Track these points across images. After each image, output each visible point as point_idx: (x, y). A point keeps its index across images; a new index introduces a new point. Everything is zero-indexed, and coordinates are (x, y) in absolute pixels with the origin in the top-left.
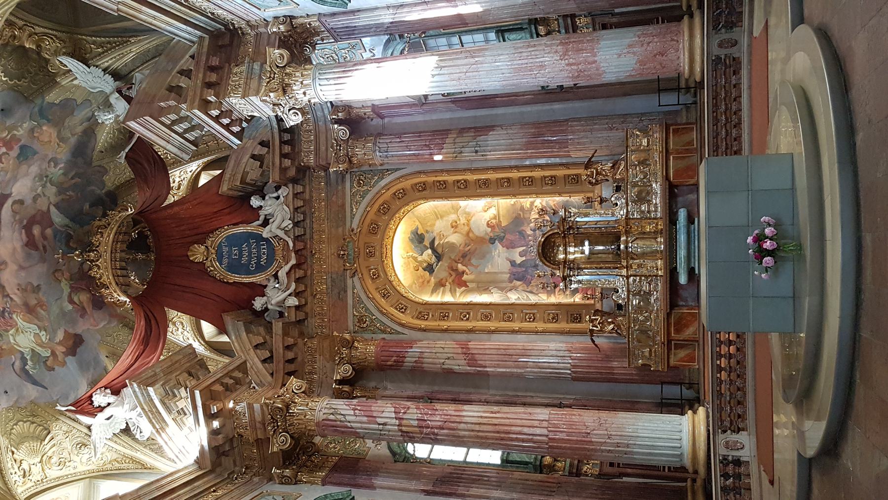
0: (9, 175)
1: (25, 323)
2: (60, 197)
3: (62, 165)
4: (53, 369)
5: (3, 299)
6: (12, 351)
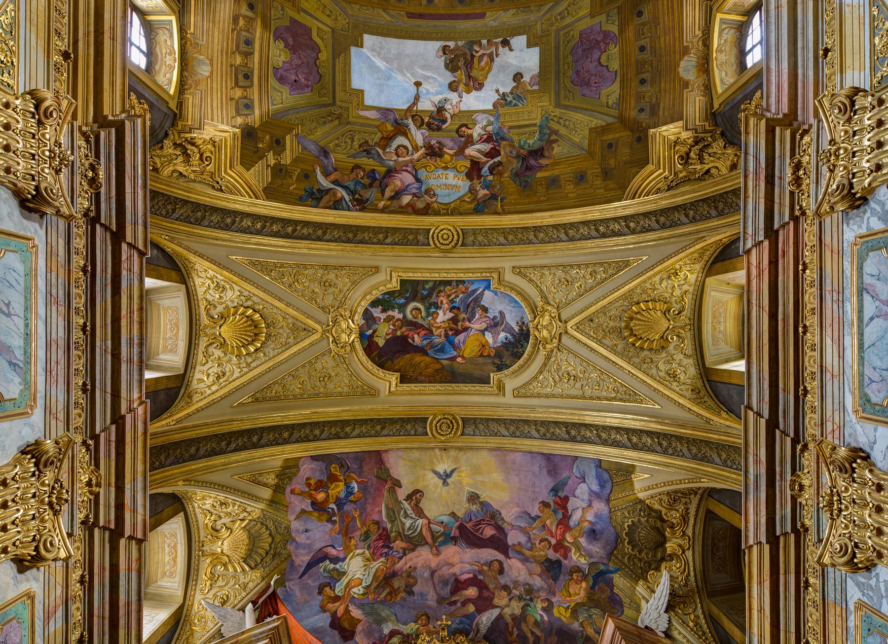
0: (528, 553)
1: (374, 570)
2: (509, 619)
3: (546, 618)
4: (320, 593)
5: (401, 548)
6: (348, 549)
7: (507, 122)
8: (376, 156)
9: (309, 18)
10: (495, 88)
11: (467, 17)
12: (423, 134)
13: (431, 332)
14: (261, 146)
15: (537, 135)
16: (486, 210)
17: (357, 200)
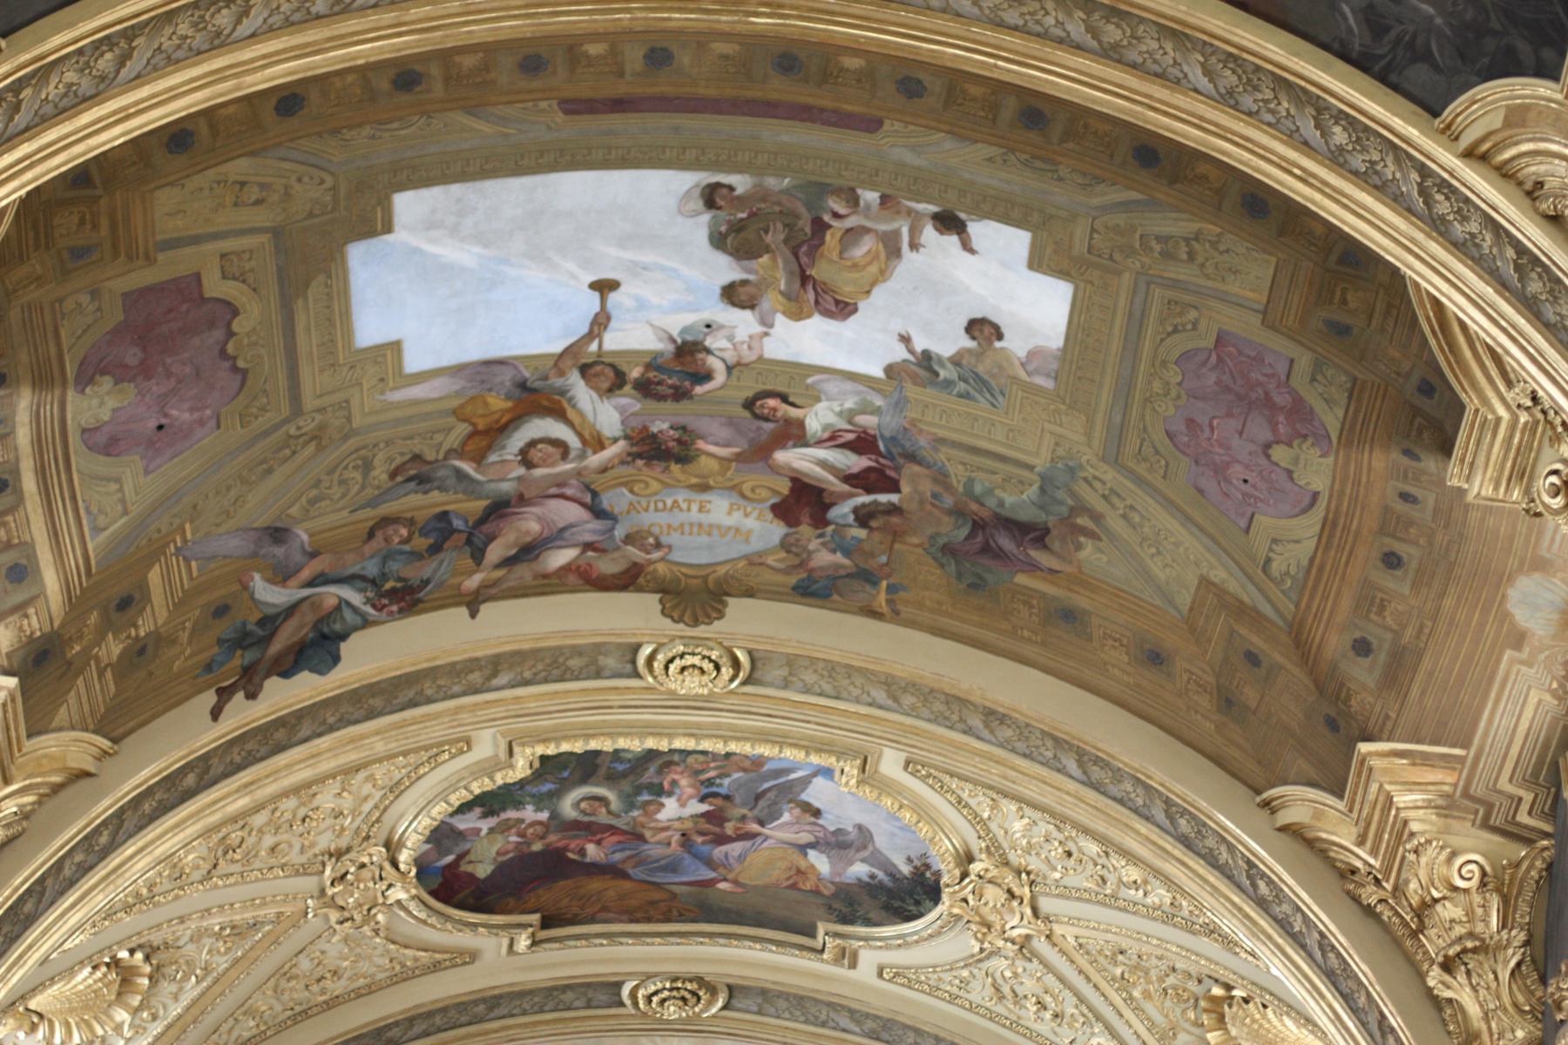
7: (929, 424)
8: (451, 481)
9: (188, 250)
10: (898, 326)
11: (804, 114)
12: (621, 410)
13: (641, 838)
14: (77, 648)
15: (1032, 492)
16: (835, 597)
17: (392, 593)
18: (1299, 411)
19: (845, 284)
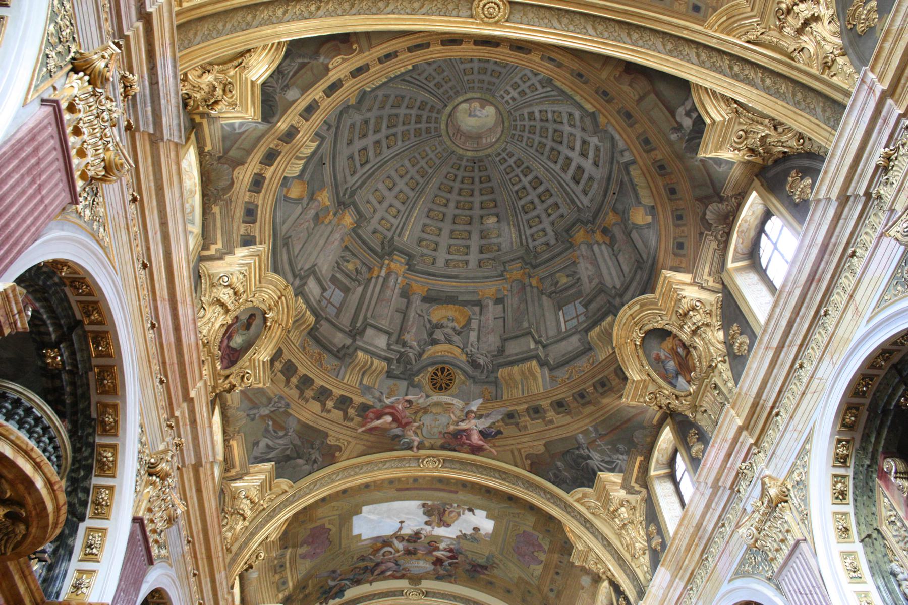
18: (540, 546)
19: (449, 522)
